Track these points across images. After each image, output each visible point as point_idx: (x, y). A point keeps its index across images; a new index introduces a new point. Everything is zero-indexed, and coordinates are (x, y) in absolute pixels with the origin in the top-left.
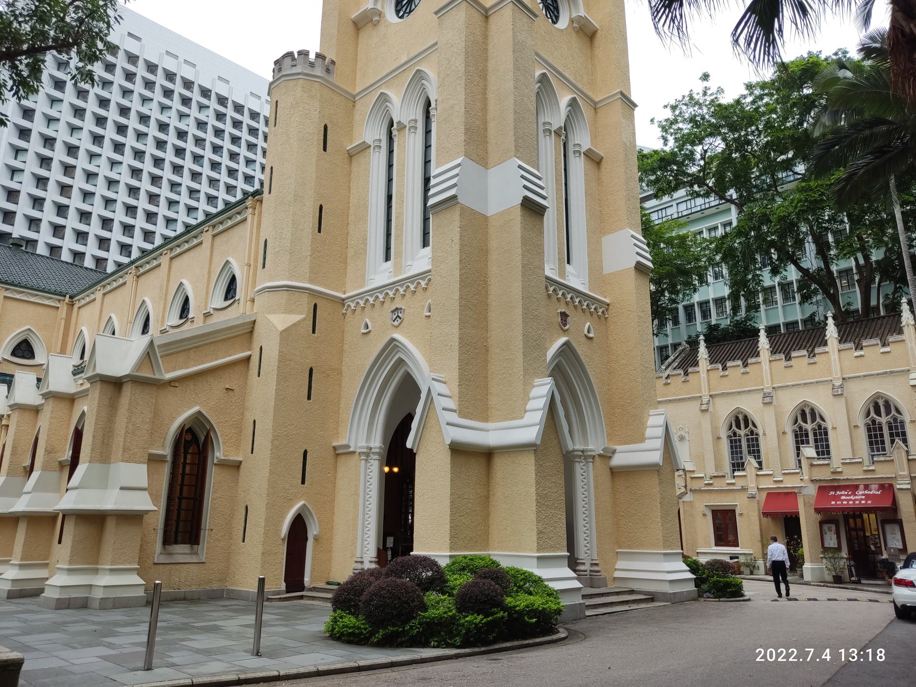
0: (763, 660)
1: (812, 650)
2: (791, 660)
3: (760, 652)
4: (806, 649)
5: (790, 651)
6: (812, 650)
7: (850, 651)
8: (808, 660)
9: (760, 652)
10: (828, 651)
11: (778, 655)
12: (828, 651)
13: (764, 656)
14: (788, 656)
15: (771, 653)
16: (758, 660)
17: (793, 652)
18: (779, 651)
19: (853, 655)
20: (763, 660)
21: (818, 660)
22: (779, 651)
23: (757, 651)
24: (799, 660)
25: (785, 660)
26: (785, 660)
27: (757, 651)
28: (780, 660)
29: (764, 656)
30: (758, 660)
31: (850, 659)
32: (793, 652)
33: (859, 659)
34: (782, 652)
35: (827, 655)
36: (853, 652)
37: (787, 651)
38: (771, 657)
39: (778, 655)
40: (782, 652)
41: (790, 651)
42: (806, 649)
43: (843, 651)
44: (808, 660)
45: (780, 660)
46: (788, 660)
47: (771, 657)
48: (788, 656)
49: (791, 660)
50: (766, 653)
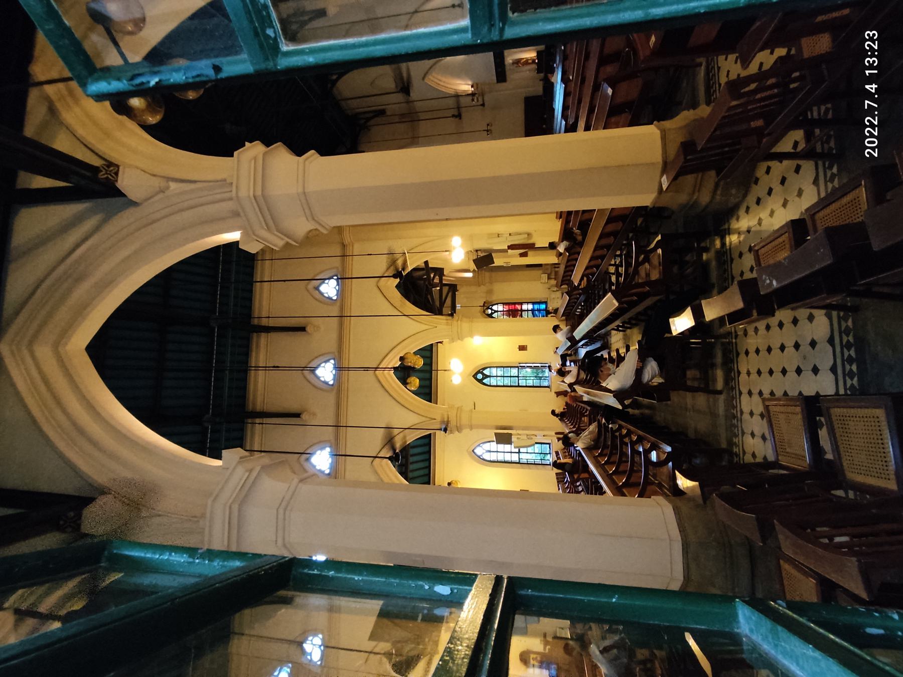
0: (876, 150)
1: (867, 102)
2: (876, 123)
3: (869, 153)
4: (866, 108)
5: (868, 124)
6: (867, 102)
7: (867, 64)
8: (876, 106)
9: (869, 153)
10: (867, 87)
11: (872, 135)
12: (867, 87)
13: (873, 149)
14: (872, 126)
16: (876, 155)
17: (869, 121)
18: (868, 135)
19: (871, 62)
20: (876, 150)
21: (876, 96)
22: (868, 135)
23: (868, 156)
24: (876, 115)
25: (876, 128)
26: (876, 128)
27: (868, 156)
28: (876, 134)
29: (873, 149)
30: (876, 155)
31: (875, 64)
32: (869, 121)
33: (875, 56)
34: (869, 132)
35: (872, 88)
36: (868, 62)
37: (868, 126)
38: (874, 142)
39: (872, 135)
40: (869, 132)
41: (868, 124)
42: (866, 108)
43: (867, 72)
44: (876, 106)
45: (876, 134)
46: (876, 126)
47: (874, 142)
48: (872, 126)
49: (876, 123)
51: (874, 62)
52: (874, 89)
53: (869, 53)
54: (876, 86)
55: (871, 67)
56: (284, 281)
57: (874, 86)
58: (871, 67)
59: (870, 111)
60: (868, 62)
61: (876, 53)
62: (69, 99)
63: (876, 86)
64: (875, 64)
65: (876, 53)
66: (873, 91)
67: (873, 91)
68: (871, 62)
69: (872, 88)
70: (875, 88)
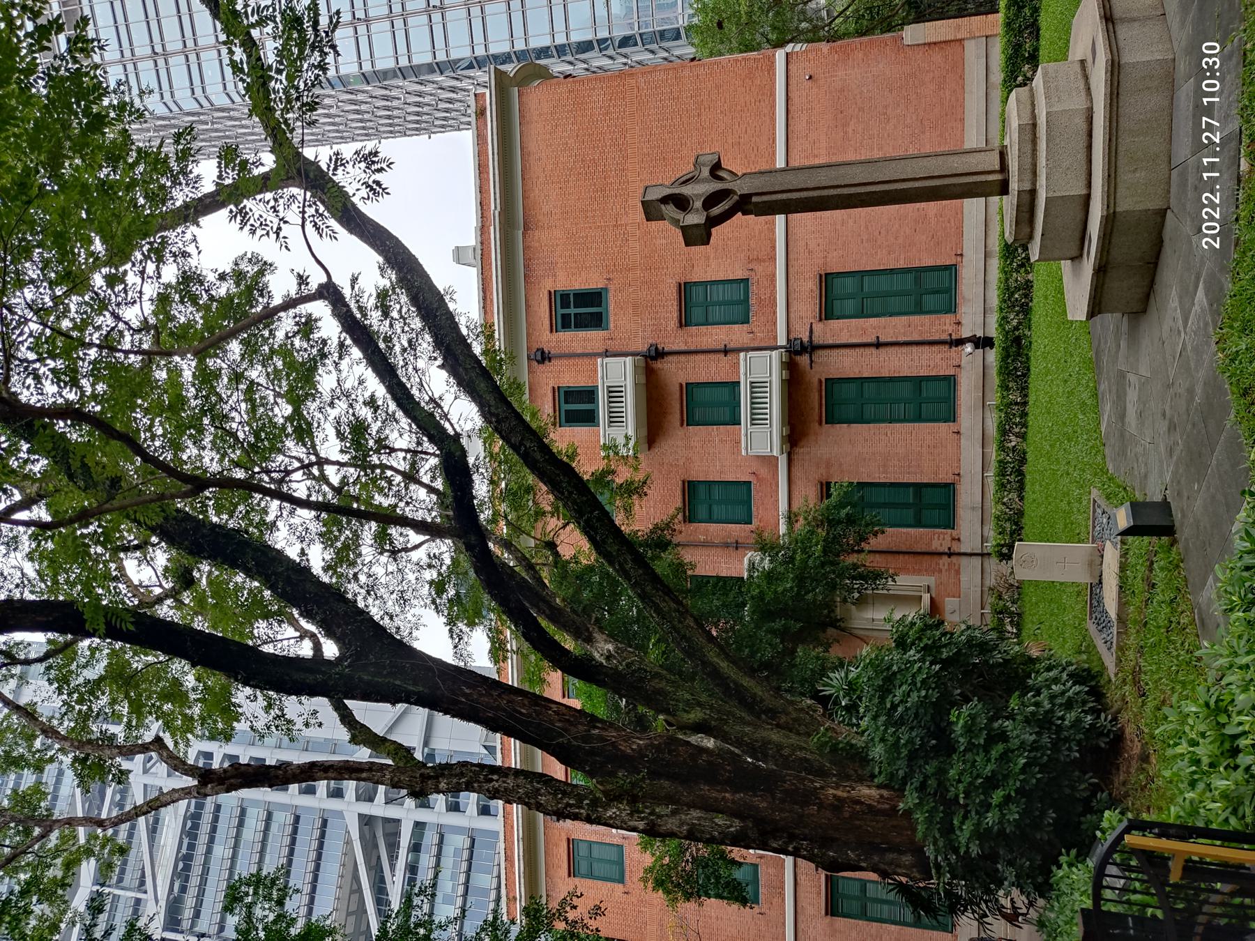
2: (1217, 201)
3: (1207, 243)
5: (1206, 202)
9: (1207, 243)
11: (1212, 219)
13: (1214, 237)
14: (1212, 205)
15: (1208, 228)
16: (1217, 246)
17: (1207, 198)
18: (1206, 217)
22: (1206, 217)
23: (1206, 247)
24: (1218, 190)
27: (1206, 247)
28: (1217, 216)
29: (1214, 237)
30: (1217, 246)
32: (1207, 198)
34: (1207, 213)
37: (1205, 206)
38: (1215, 228)
39: (1212, 219)
40: (1207, 213)
41: (1206, 202)
45: (1217, 216)
47: (1215, 228)
48: (1212, 205)
49: (1217, 201)
50: (1207, 236)
59: (1210, 186)
61: (1218, 74)
65: (1218, 74)
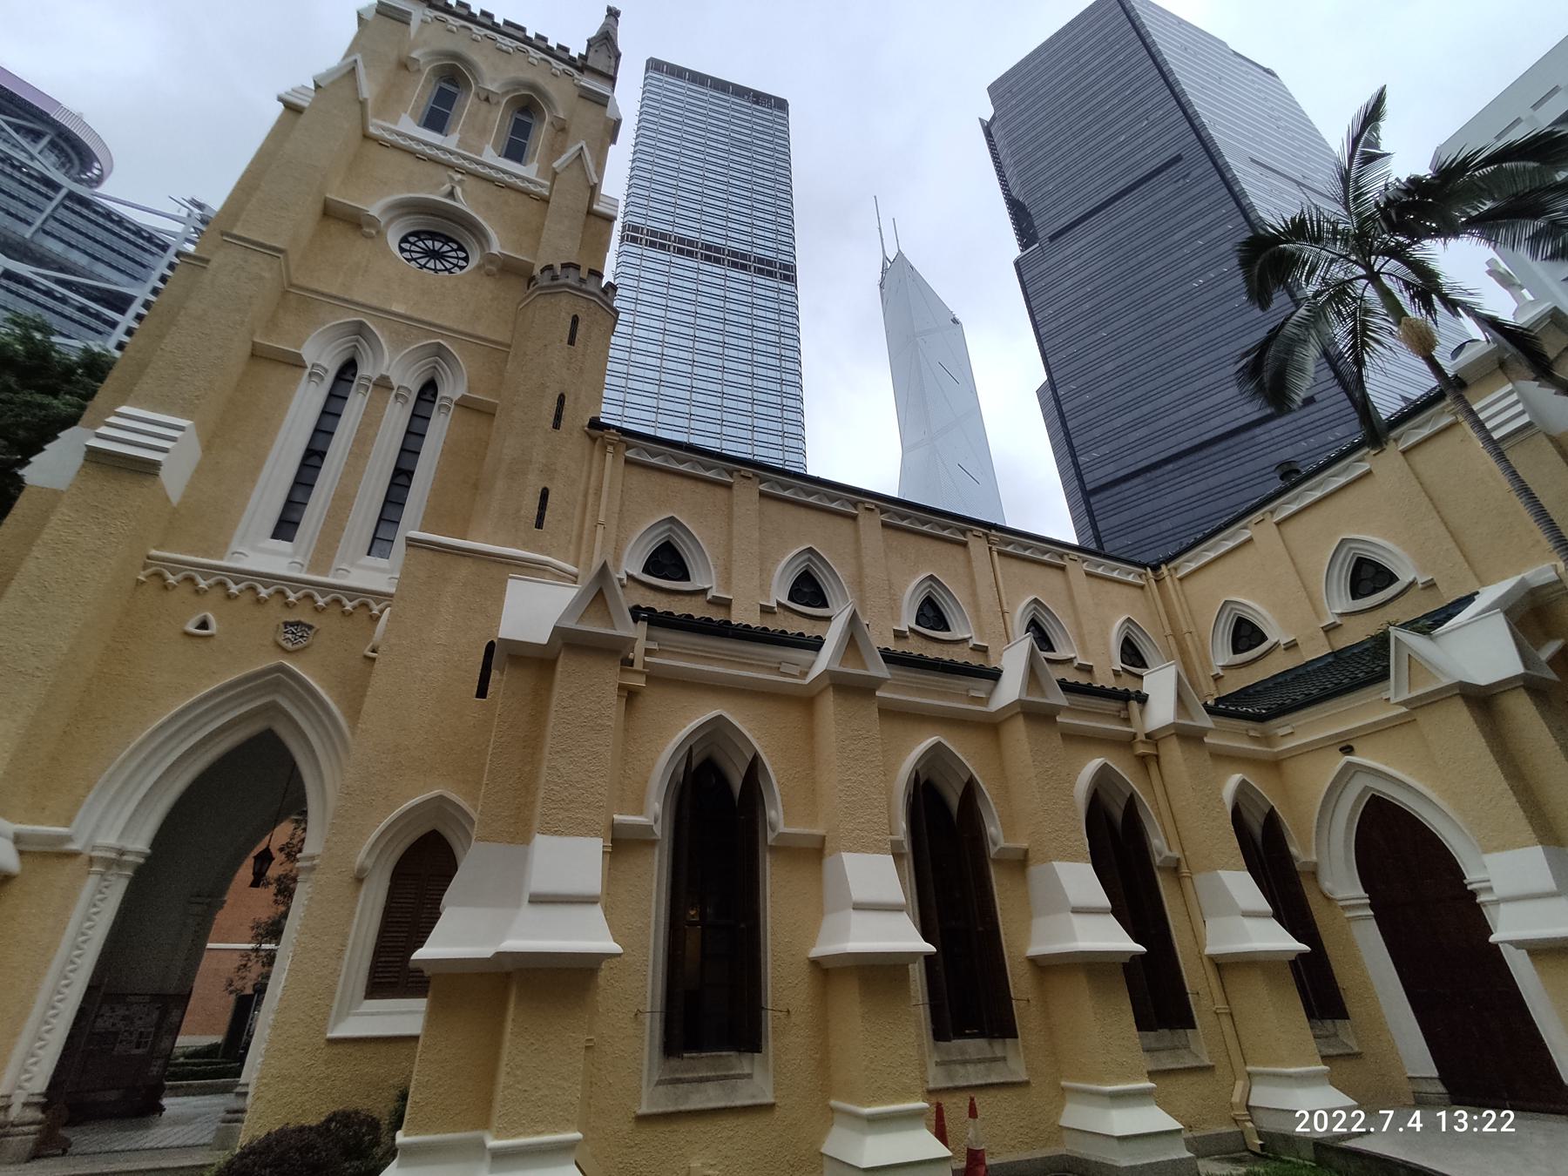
51: (1461, 1126)
52: (1414, 1125)
53: (1475, 1117)
54: (1418, 1130)
55: (1452, 1121)
56: (882, 239)
57: (1418, 1126)
58: (1452, 1121)
60: (1461, 1116)
62: (1493, 243)
63: (1418, 1130)
64: (1456, 1128)
66: (1410, 1125)
67: (1410, 1125)
68: (1460, 1121)
69: (1415, 1122)
70: (1415, 1128)
